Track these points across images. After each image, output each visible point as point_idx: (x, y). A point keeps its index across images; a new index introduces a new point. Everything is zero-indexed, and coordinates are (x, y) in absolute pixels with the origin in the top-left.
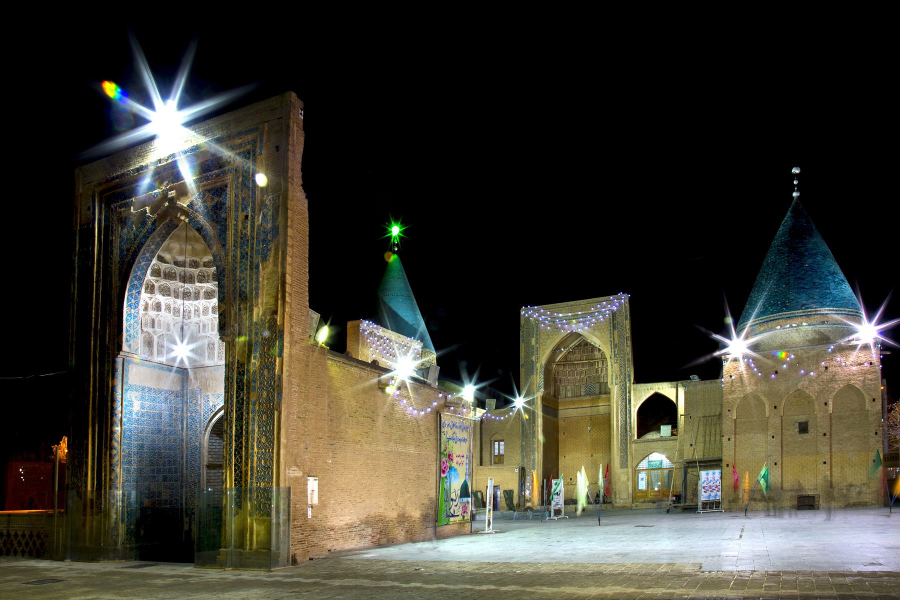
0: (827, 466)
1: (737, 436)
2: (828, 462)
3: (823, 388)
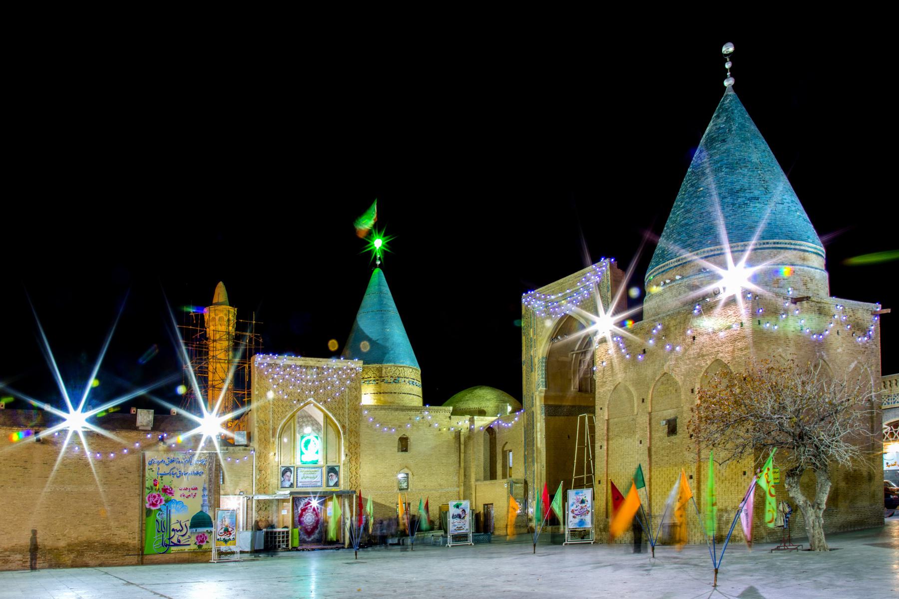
0: (694, 483)
1: (610, 442)
2: (695, 477)
3: (690, 368)
